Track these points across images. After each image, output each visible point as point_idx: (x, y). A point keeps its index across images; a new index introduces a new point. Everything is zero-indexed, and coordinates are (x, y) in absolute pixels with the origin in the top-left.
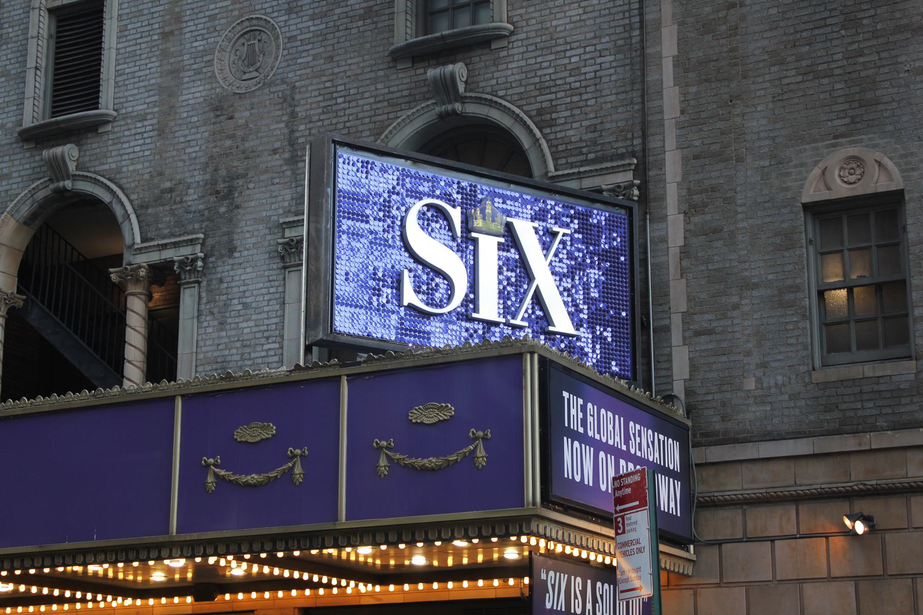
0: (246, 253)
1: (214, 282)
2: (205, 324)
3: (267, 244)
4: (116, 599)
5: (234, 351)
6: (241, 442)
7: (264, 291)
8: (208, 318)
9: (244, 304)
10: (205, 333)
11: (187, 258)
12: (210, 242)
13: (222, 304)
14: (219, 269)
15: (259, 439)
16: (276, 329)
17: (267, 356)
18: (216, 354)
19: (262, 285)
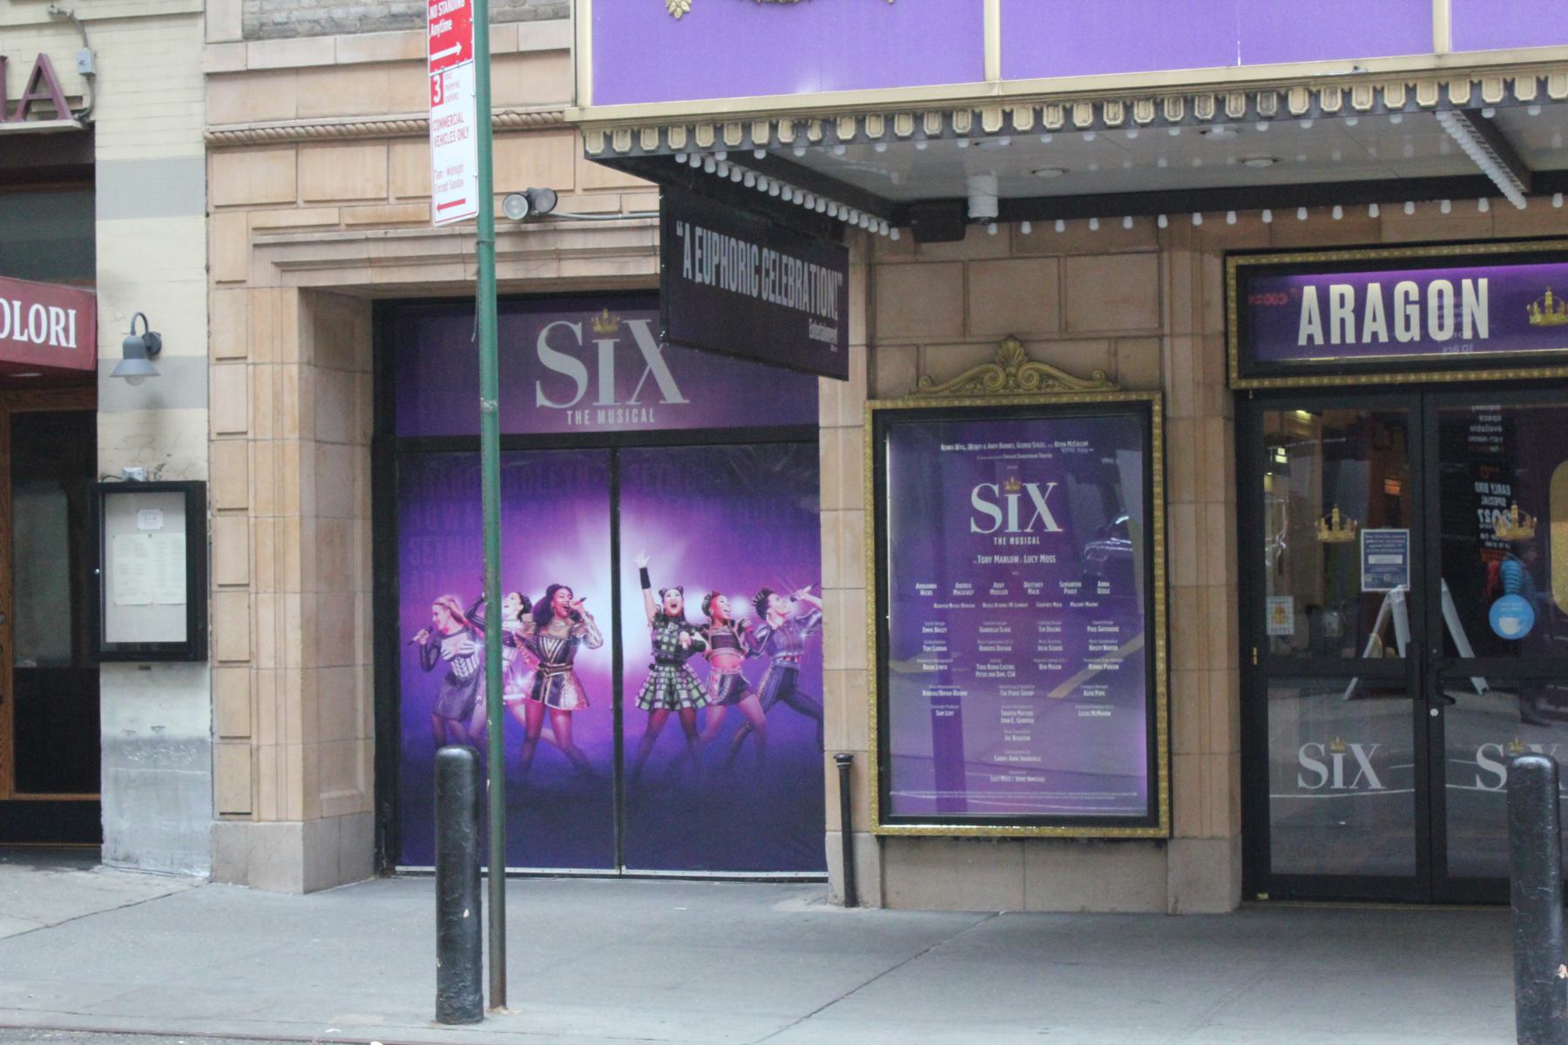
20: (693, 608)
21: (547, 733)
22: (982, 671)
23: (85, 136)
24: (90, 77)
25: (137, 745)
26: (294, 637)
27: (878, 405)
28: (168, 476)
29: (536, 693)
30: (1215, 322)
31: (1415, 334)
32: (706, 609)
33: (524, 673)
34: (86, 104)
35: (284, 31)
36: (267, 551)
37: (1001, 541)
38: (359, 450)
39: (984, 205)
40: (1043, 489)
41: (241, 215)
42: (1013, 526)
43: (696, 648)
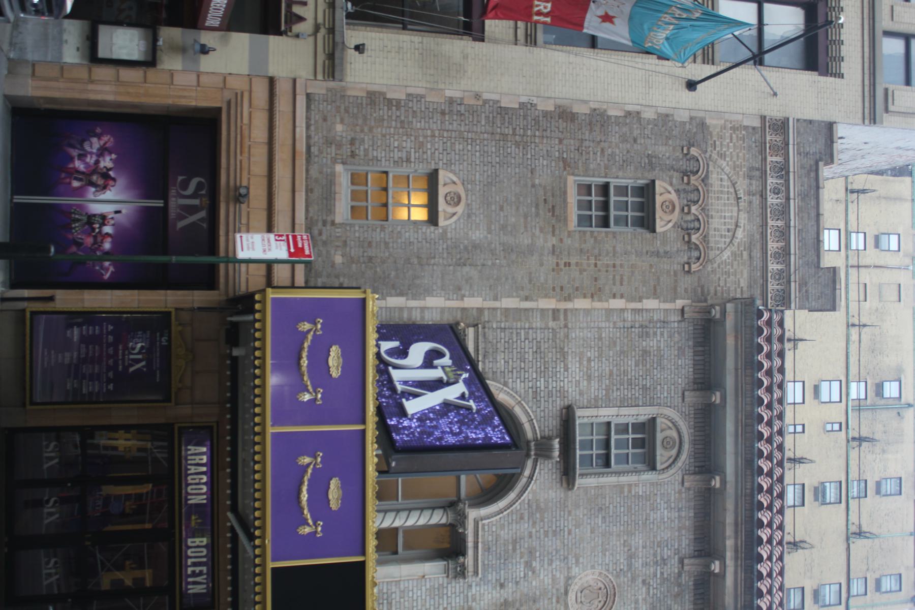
20: (107, 229)
21: (63, 175)
22: (83, 346)
23: (279, 33)
24: (297, 36)
25: (61, 32)
26: (99, 97)
27: (173, 314)
28: (159, 53)
29: (77, 171)
31: (190, 481)
32: (107, 234)
33: (85, 168)
34: (289, 34)
35: (308, 108)
37: (127, 352)
39: (236, 352)
40: (143, 367)
41: (248, 88)
42: (132, 357)
43: (94, 229)
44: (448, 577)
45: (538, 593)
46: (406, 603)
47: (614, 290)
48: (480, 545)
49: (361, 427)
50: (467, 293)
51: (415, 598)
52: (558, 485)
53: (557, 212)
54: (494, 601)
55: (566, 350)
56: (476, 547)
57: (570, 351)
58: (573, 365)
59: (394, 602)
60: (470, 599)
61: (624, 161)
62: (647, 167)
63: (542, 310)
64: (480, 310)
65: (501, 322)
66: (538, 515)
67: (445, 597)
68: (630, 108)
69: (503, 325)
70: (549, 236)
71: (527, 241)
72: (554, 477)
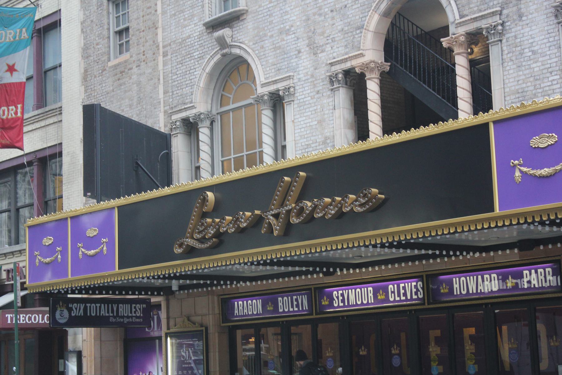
0: (530, 16)
1: (511, 39)
2: (508, 68)
3: (544, 8)
4: (469, 254)
5: (529, 84)
6: (535, 147)
7: (545, 41)
8: (509, 64)
9: (533, 51)
10: (509, 74)
11: (491, 26)
12: (505, 12)
13: (517, 53)
14: (513, 30)
15: (546, 145)
16: (556, 66)
17: (552, 85)
18: (517, 87)
19: (543, 37)
30: (217, 311)
36: (89, 366)
38: (119, 342)
39: (175, 288)
44: (293, 101)
45: (304, 18)
46: (308, 132)
47: (153, 12)
48: (273, 79)
49: (69, 220)
50: (158, 125)
51: (304, 126)
52: (245, 22)
53: (122, 69)
54: (308, 56)
55: (180, 40)
56: (275, 82)
57: (181, 37)
58: (187, 31)
59: (307, 143)
60: (306, 78)
61: (101, 27)
62: (101, 8)
63: (163, 66)
64: (165, 112)
65: (169, 96)
66: (261, 34)
67: (305, 100)
68: (80, 30)
69: (171, 94)
70: (132, 71)
71: (135, 87)
72: (241, 27)
